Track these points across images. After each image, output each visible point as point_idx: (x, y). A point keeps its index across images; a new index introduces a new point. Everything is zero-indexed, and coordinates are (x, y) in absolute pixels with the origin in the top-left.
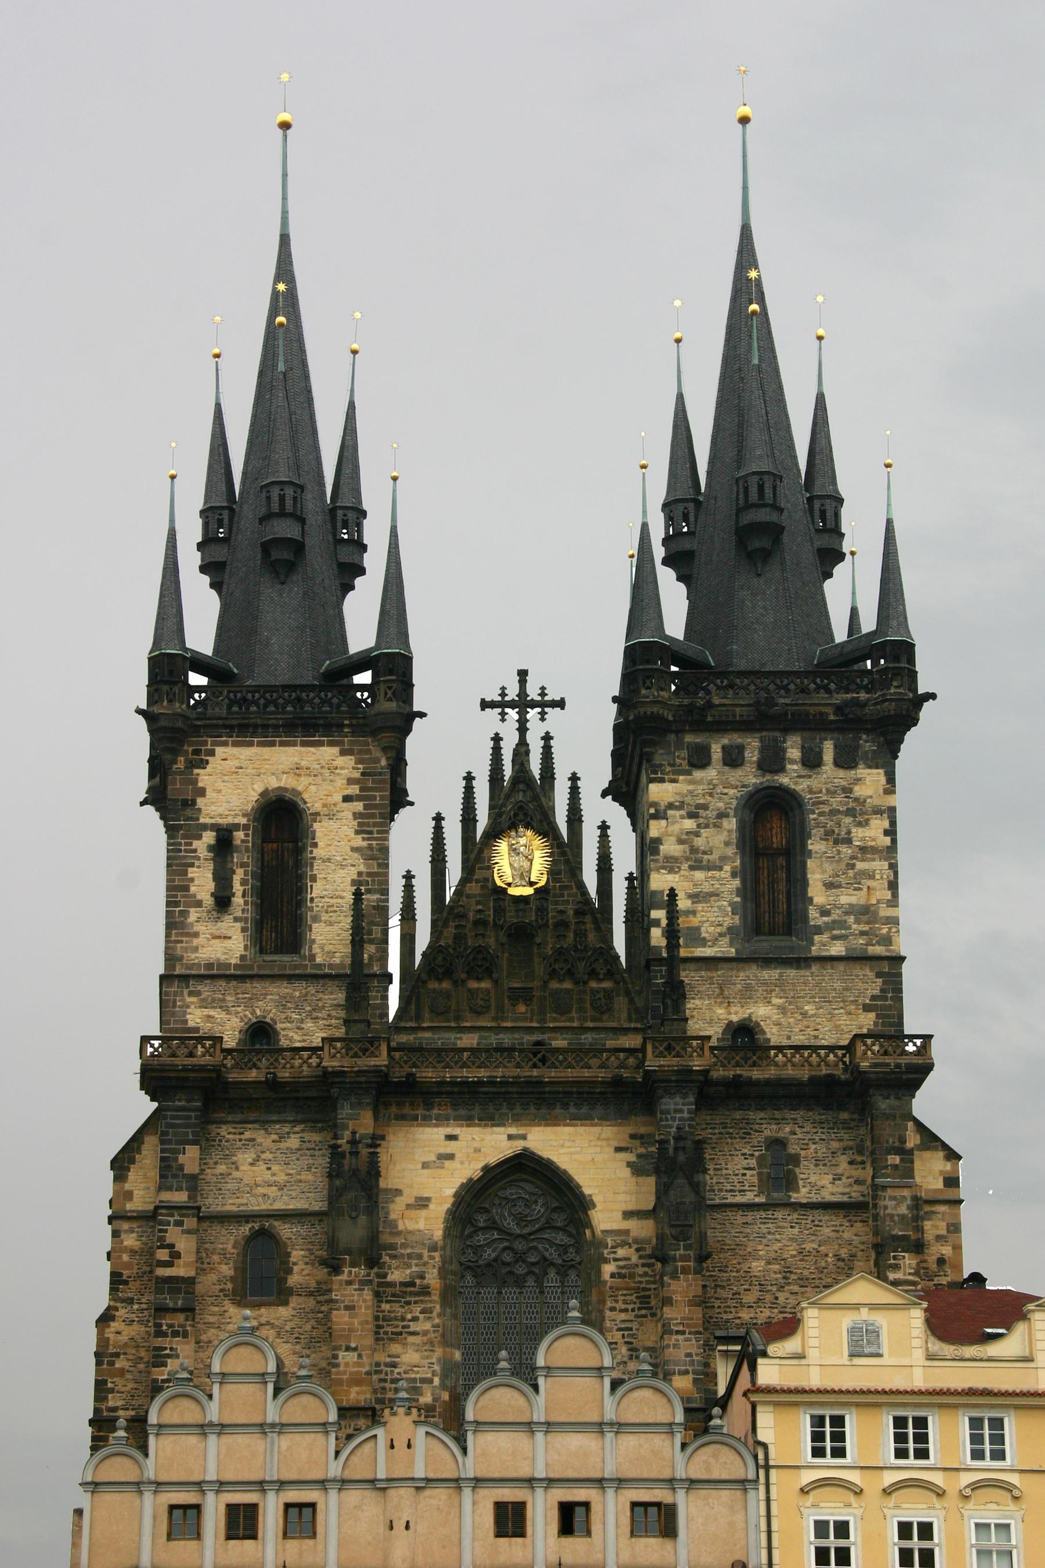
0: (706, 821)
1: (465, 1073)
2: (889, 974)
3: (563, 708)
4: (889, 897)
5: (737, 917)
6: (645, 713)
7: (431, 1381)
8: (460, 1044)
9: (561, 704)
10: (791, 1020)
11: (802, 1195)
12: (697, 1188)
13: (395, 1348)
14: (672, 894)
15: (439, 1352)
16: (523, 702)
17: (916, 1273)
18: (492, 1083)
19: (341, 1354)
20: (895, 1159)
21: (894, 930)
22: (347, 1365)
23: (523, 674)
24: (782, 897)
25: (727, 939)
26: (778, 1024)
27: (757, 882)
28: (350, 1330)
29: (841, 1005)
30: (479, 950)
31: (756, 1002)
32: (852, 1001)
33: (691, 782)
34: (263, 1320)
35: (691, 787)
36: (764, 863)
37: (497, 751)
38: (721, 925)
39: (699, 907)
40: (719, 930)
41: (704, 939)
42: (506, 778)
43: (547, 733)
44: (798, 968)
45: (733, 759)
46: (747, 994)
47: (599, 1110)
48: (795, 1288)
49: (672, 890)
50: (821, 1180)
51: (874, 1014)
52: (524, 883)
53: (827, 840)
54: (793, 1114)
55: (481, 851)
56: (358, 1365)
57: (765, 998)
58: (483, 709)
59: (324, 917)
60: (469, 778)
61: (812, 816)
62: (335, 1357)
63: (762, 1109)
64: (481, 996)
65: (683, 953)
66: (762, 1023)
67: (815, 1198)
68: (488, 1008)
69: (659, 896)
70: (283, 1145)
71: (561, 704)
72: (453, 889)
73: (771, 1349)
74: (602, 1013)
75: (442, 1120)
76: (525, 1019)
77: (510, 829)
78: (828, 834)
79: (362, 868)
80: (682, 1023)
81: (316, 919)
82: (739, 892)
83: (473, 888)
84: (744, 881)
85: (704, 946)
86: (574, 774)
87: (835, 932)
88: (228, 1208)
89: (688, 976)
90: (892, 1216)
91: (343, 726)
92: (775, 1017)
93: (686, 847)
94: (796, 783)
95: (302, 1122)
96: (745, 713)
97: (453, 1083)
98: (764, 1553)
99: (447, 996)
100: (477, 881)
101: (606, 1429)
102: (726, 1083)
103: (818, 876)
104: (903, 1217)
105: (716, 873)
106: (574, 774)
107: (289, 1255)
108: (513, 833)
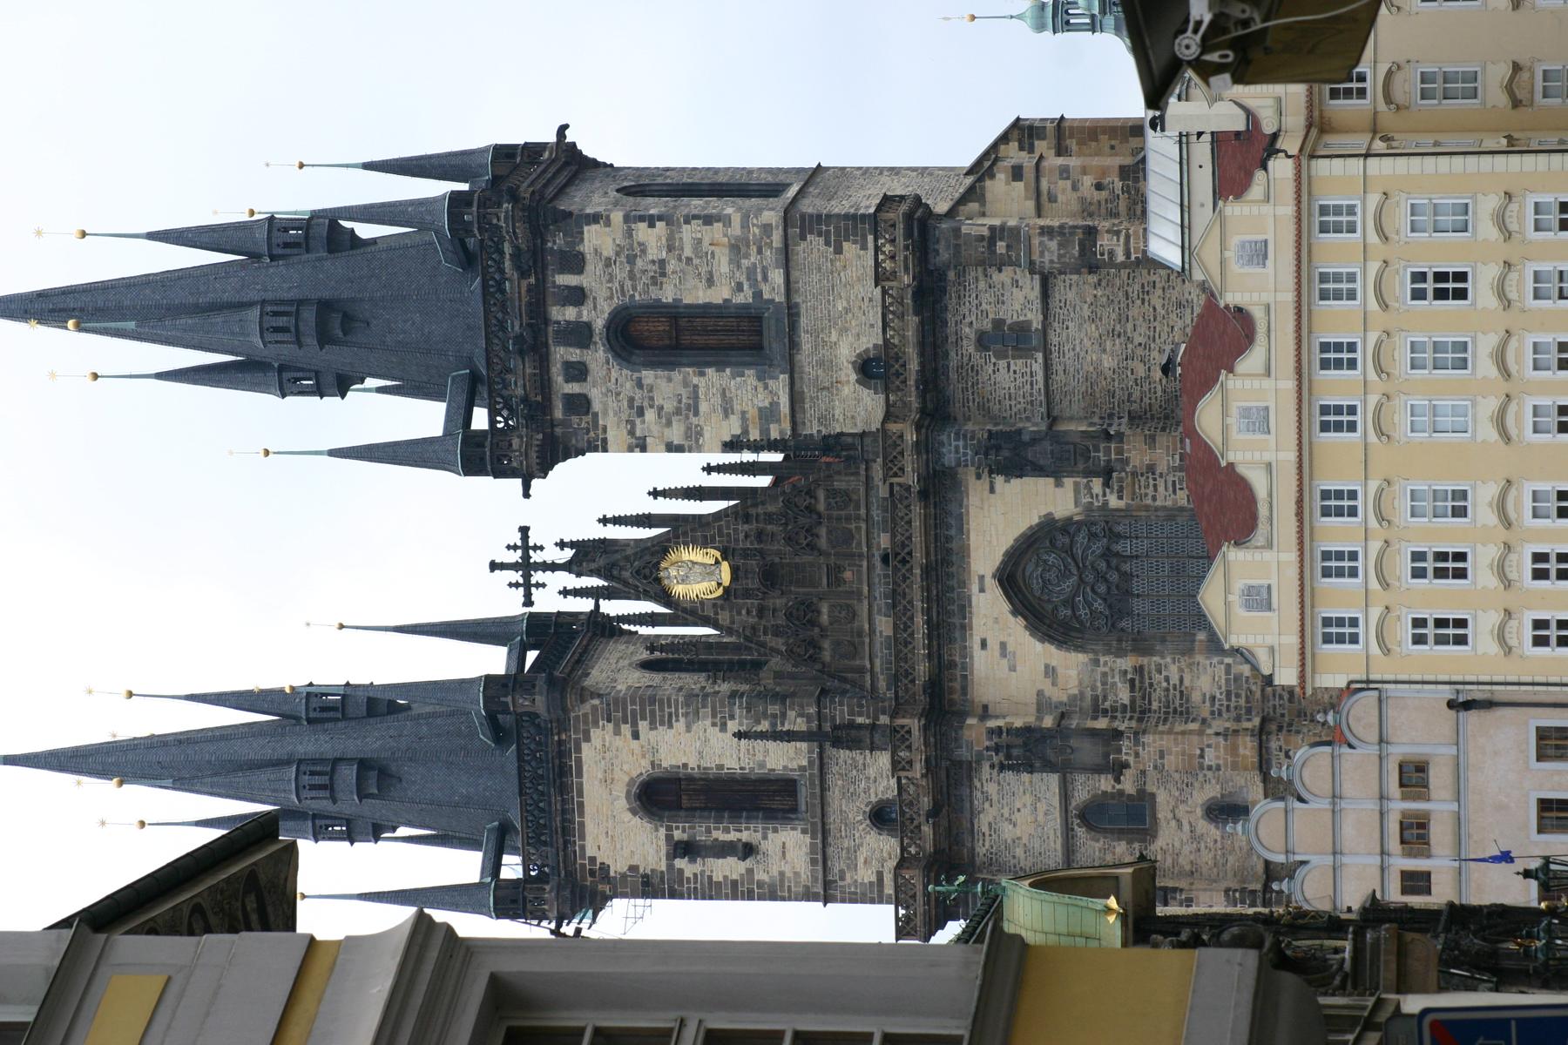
1: (919, 636)
2: (802, 228)
7: (1228, 666)
9: (524, 531)
11: (1035, 318)
12: (1036, 440)
13: (1196, 697)
15: (1199, 658)
17: (1118, 233)
18: (928, 612)
19: (1207, 762)
20: (1001, 247)
22: (1218, 757)
23: (494, 566)
25: (770, 382)
28: (1183, 754)
30: (789, 616)
33: (605, 413)
34: (1170, 816)
35: (611, 413)
36: (686, 339)
39: (737, 408)
40: (760, 389)
44: (798, 314)
45: (578, 372)
46: (828, 365)
47: (953, 507)
48: (1130, 326)
50: (1016, 298)
51: (846, 245)
55: (685, 610)
56: (1217, 747)
59: (759, 757)
62: (1210, 768)
63: (947, 354)
67: (1037, 305)
68: (848, 606)
70: (995, 798)
71: (524, 531)
73: (1266, 671)
75: (965, 652)
76: (859, 572)
79: (708, 722)
81: (762, 765)
82: (720, 369)
83: (724, 618)
84: (709, 365)
86: (600, 521)
87: (759, 278)
88: (1059, 847)
89: (812, 428)
90: (1060, 256)
91: (560, 741)
93: (675, 419)
94: (602, 312)
95: (971, 780)
97: (929, 647)
98: (1440, 687)
99: (837, 644)
100: (716, 613)
101: (1337, 808)
102: (922, 395)
103: (701, 294)
104: (1060, 245)
105: (701, 391)
106: (600, 521)
107: (1104, 793)
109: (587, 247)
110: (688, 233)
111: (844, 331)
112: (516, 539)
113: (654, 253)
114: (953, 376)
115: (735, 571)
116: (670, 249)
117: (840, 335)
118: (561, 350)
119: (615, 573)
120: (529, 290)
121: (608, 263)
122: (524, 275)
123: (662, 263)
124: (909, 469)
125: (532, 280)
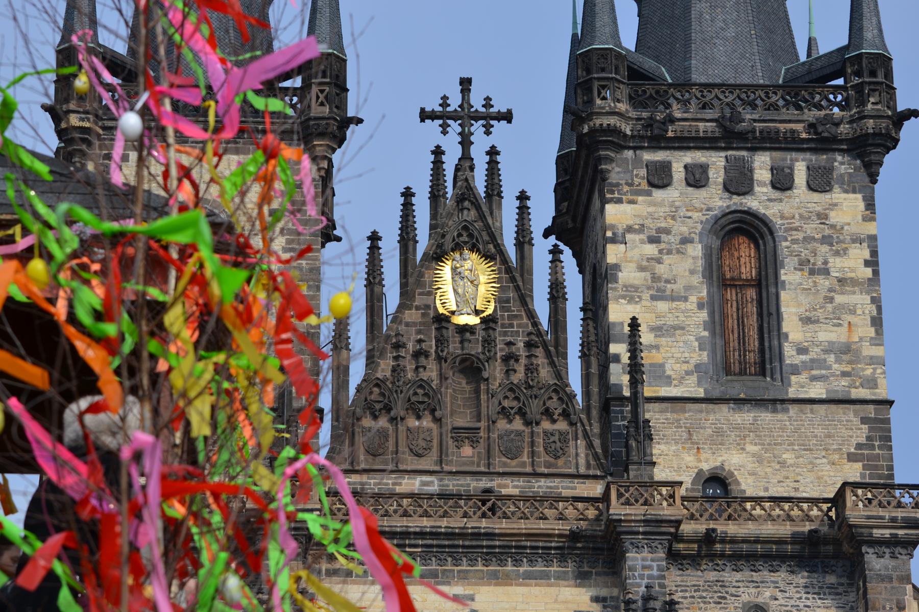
0: (668, 247)
2: (876, 420)
3: (509, 121)
4: (873, 334)
5: (705, 353)
6: (601, 125)
8: (398, 489)
9: (507, 117)
10: (768, 470)
14: (634, 324)
16: (465, 114)
21: (879, 371)
23: (466, 84)
24: (753, 334)
25: (694, 378)
26: (753, 474)
27: (724, 316)
29: (823, 453)
31: (729, 449)
32: (835, 450)
33: (652, 204)
35: (651, 209)
36: (731, 294)
37: (438, 164)
38: (687, 362)
39: (663, 341)
40: (685, 367)
41: (669, 377)
42: (449, 195)
43: (493, 147)
44: (775, 411)
45: (697, 178)
46: (718, 439)
49: (634, 319)
51: (860, 464)
52: (469, 311)
53: (803, 270)
54: (774, 577)
55: (421, 275)
57: (738, 444)
58: (422, 120)
60: (408, 194)
61: (784, 244)
64: (422, 436)
65: (648, 392)
66: (736, 473)
69: (618, 328)
71: (507, 117)
72: (390, 318)
74: (557, 457)
77: (453, 250)
78: (803, 263)
80: (648, 468)
84: (712, 314)
85: (669, 384)
87: (814, 372)
92: (750, 466)
93: (648, 275)
94: (767, 208)
96: (710, 130)
99: (383, 434)
100: (418, 308)
103: (794, 310)
105: (682, 305)
108: (457, 255)
109: (837, 195)
110: (861, 300)
111: (760, 461)
112: (499, 106)
113: (836, 264)
114: (712, 576)
115: (464, 329)
116: (840, 281)
117: (754, 455)
118: (722, 163)
119: (466, 204)
120: (793, 131)
121: (822, 217)
122: (812, 126)
123: (826, 272)
124: (628, 510)
125: (804, 136)
